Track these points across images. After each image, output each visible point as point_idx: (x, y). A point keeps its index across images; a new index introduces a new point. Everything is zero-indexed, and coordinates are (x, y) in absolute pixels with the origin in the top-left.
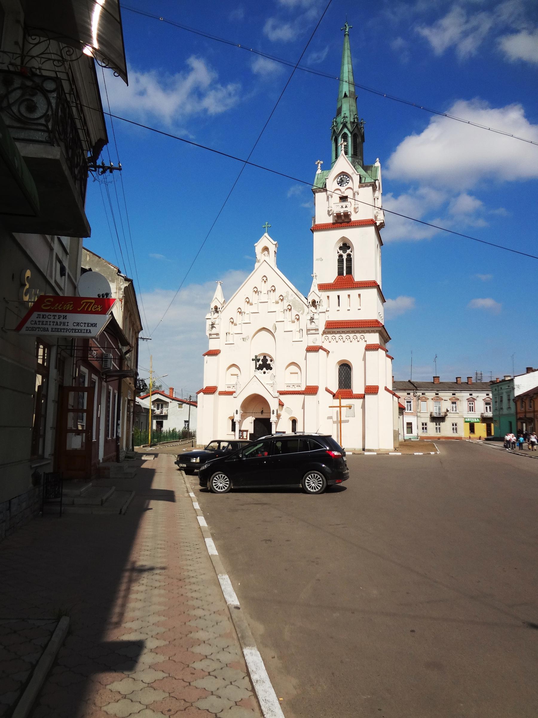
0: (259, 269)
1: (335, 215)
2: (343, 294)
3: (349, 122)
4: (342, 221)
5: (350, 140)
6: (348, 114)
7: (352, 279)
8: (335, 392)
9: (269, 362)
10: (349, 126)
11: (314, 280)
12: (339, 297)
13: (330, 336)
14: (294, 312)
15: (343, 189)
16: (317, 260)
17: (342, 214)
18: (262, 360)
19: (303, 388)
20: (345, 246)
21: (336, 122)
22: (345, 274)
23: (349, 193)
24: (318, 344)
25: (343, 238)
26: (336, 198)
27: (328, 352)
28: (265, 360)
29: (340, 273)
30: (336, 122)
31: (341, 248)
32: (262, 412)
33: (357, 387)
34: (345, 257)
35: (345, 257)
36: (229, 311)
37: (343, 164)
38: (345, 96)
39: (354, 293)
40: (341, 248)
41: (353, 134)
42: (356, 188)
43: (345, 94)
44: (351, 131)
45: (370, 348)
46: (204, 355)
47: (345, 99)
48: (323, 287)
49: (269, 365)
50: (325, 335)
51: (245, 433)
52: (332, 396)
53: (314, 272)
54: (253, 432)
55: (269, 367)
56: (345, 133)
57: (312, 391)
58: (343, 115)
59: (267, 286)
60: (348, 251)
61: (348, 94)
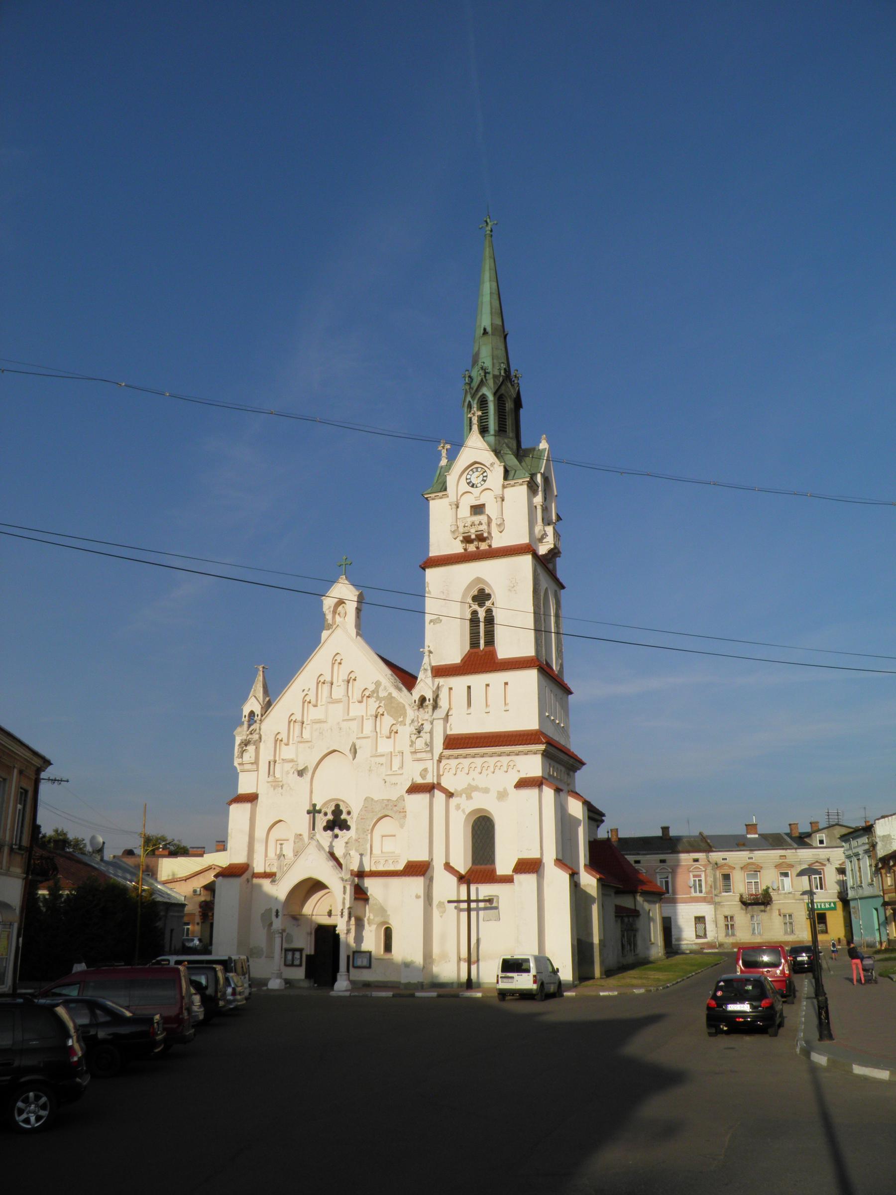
0: (329, 641)
2: (477, 681)
3: (491, 376)
4: (476, 548)
5: (491, 407)
6: (488, 364)
7: (493, 654)
8: (463, 871)
9: (344, 816)
10: (491, 382)
11: (426, 660)
12: (469, 687)
13: (453, 763)
14: (388, 721)
16: (431, 621)
17: (473, 537)
18: (333, 813)
19: (400, 867)
21: (470, 377)
23: (488, 499)
24: (430, 779)
25: (478, 580)
26: (465, 511)
27: (450, 795)
28: (337, 811)
29: (474, 643)
30: (470, 377)
31: (475, 599)
32: (330, 914)
33: (504, 864)
34: (482, 614)
35: (482, 614)
36: (274, 723)
37: (476, 448)
38: (485, 332)
39: (496, 679)
40: (475, 599)
41: (499, 394)
42: (498, 490)
43: (485, 329)
44: (494, 391)
45: (523, 784)
46: (230, 803)
47: (486, 338)
48: (441, 672)
49: (345, 821)
50: (444, 762)
51: (297, 955)
52: (454, 880)
53: (427, 643)
54: (313, 953)
55: (344, 826)
56: (483, 395)
57: (418, 869)
58: (480, 364)
59: (342, 674)
60: (488, 604)
61: (489, 329)
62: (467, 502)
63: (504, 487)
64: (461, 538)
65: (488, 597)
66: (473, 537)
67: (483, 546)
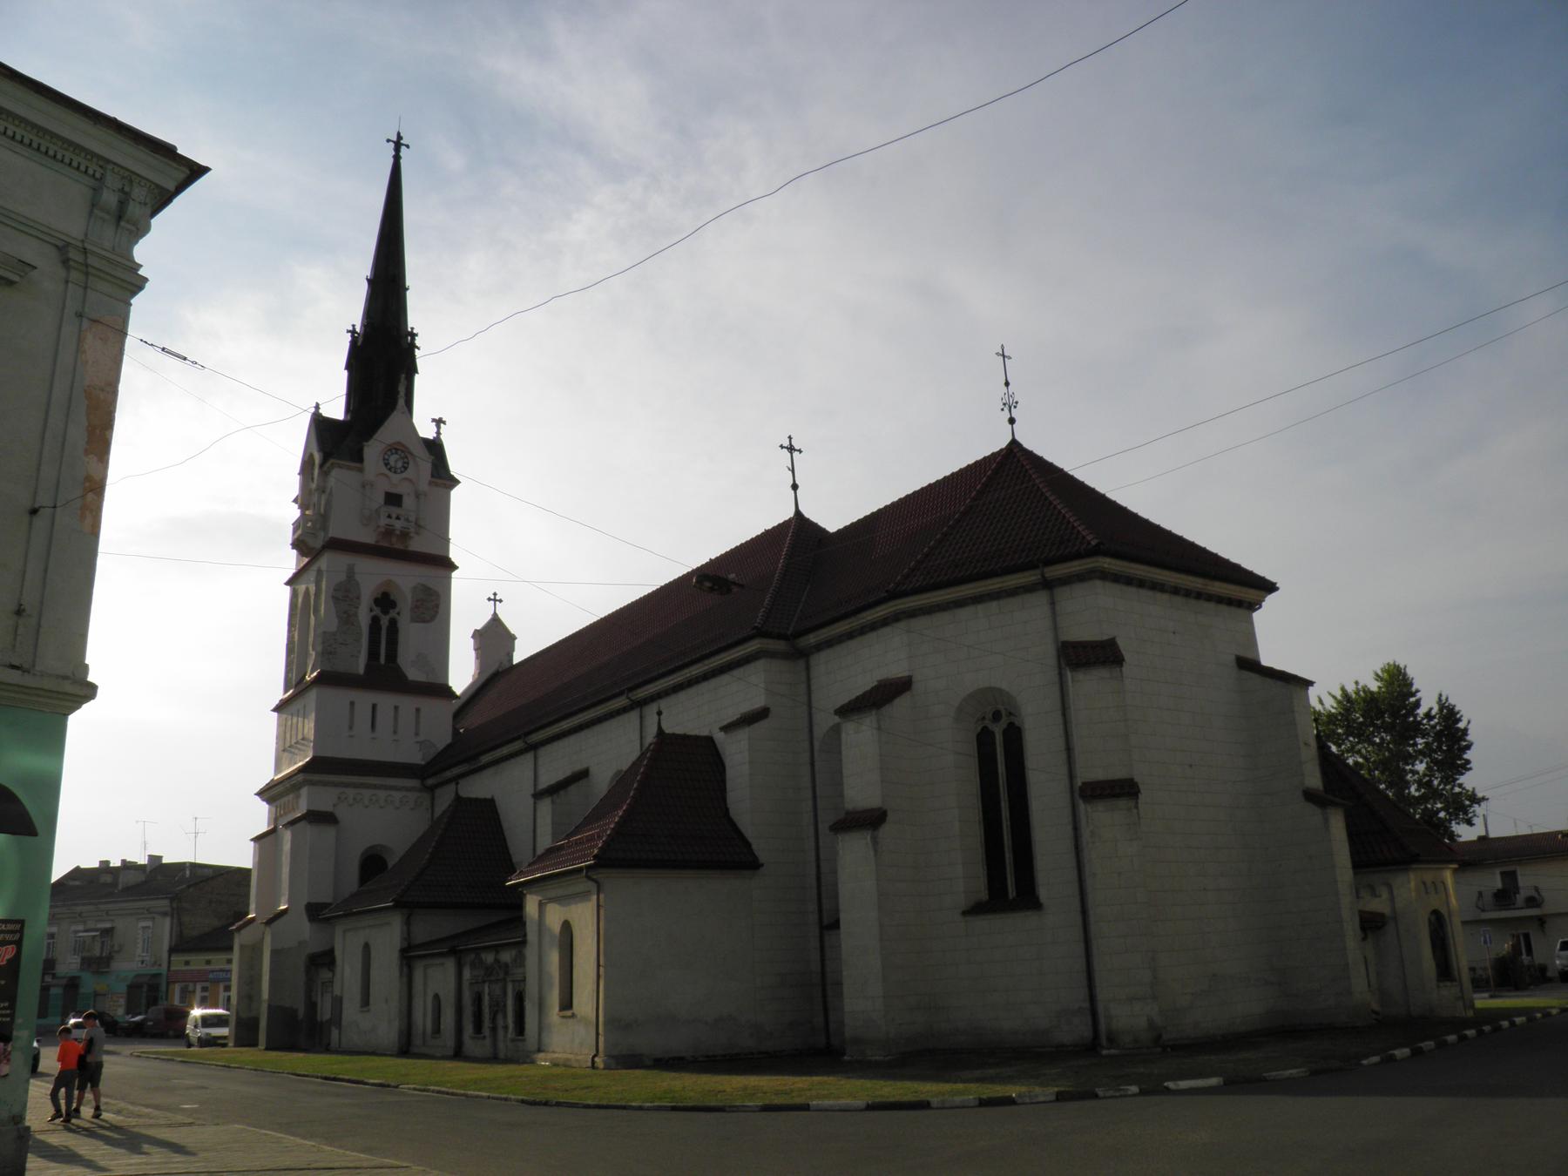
2: (386, 701)
12: (374, 707)
15: (395, 478)
22: (382, 660)
25: (389, 582)
34: (385, 622)
35: (385, 622)
40: (377, 602)
60: (393, 613)
62: (383, 486)
63: (430, 483)
65: (393, 604)
67: (399, 546)
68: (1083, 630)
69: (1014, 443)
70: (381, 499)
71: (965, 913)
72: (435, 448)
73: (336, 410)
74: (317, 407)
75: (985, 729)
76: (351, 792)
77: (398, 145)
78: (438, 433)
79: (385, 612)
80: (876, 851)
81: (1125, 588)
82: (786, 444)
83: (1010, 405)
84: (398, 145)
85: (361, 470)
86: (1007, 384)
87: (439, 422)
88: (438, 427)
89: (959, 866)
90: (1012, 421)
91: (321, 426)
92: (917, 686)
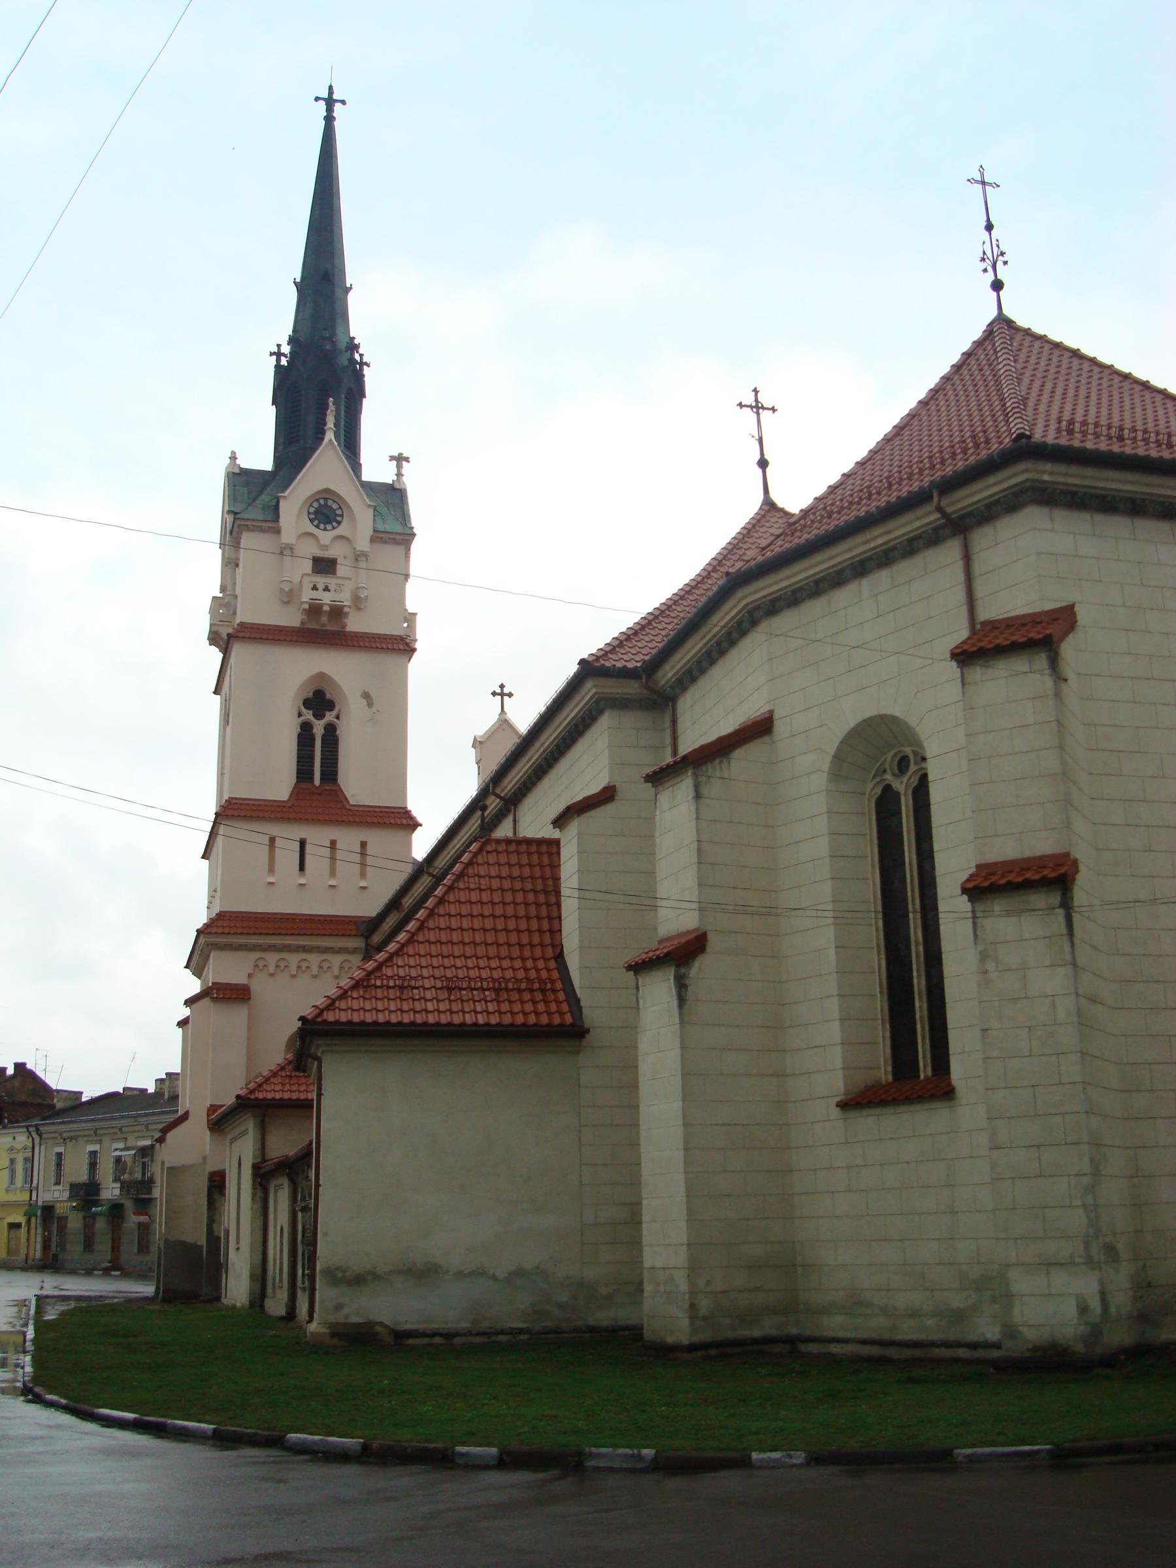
1: (306, 606)
2: (318, 837)
15: (325, 536)
17: (326, 608)
20: (319, 701)
22: (317, 781)
25: (322, 676)
34: (319, 729)
35: (319, 729)
40: (307, 703)
60: (329, 717)
62: (310, 549)
64: (306, 606)
65: (330, 705)
66: (326, 608)
68: (1012, 594)
69: (1002, 326)
70: (308, 566)
71: (844, 1106)
72: (391, 498)
73: (261, 458)
74: (233, 457)
75: (888, 788)
76: (272, 958)
77: (330, 102)
78: (399, 475)
79: (319, 716)
80: (682, 1001)
81: (1100, 518)
82: (750, 400)
83: (993, 260)
84: (330, 102)
85: (277, 531)
86: (989, 227)
87: (400, 459)
88: (399, 467)
89: (830, 1025)
90: (997, 286)
91: (242, 484)
92: (779, 727)
